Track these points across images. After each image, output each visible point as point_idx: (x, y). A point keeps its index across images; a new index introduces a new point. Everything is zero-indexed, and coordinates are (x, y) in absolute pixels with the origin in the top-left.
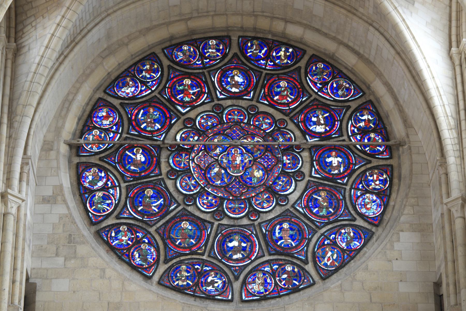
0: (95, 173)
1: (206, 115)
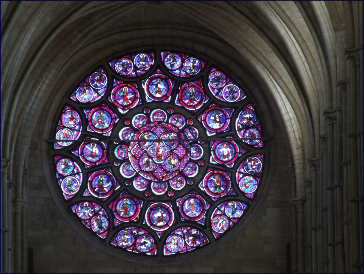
0: (66, 162)
1: (139, 116)
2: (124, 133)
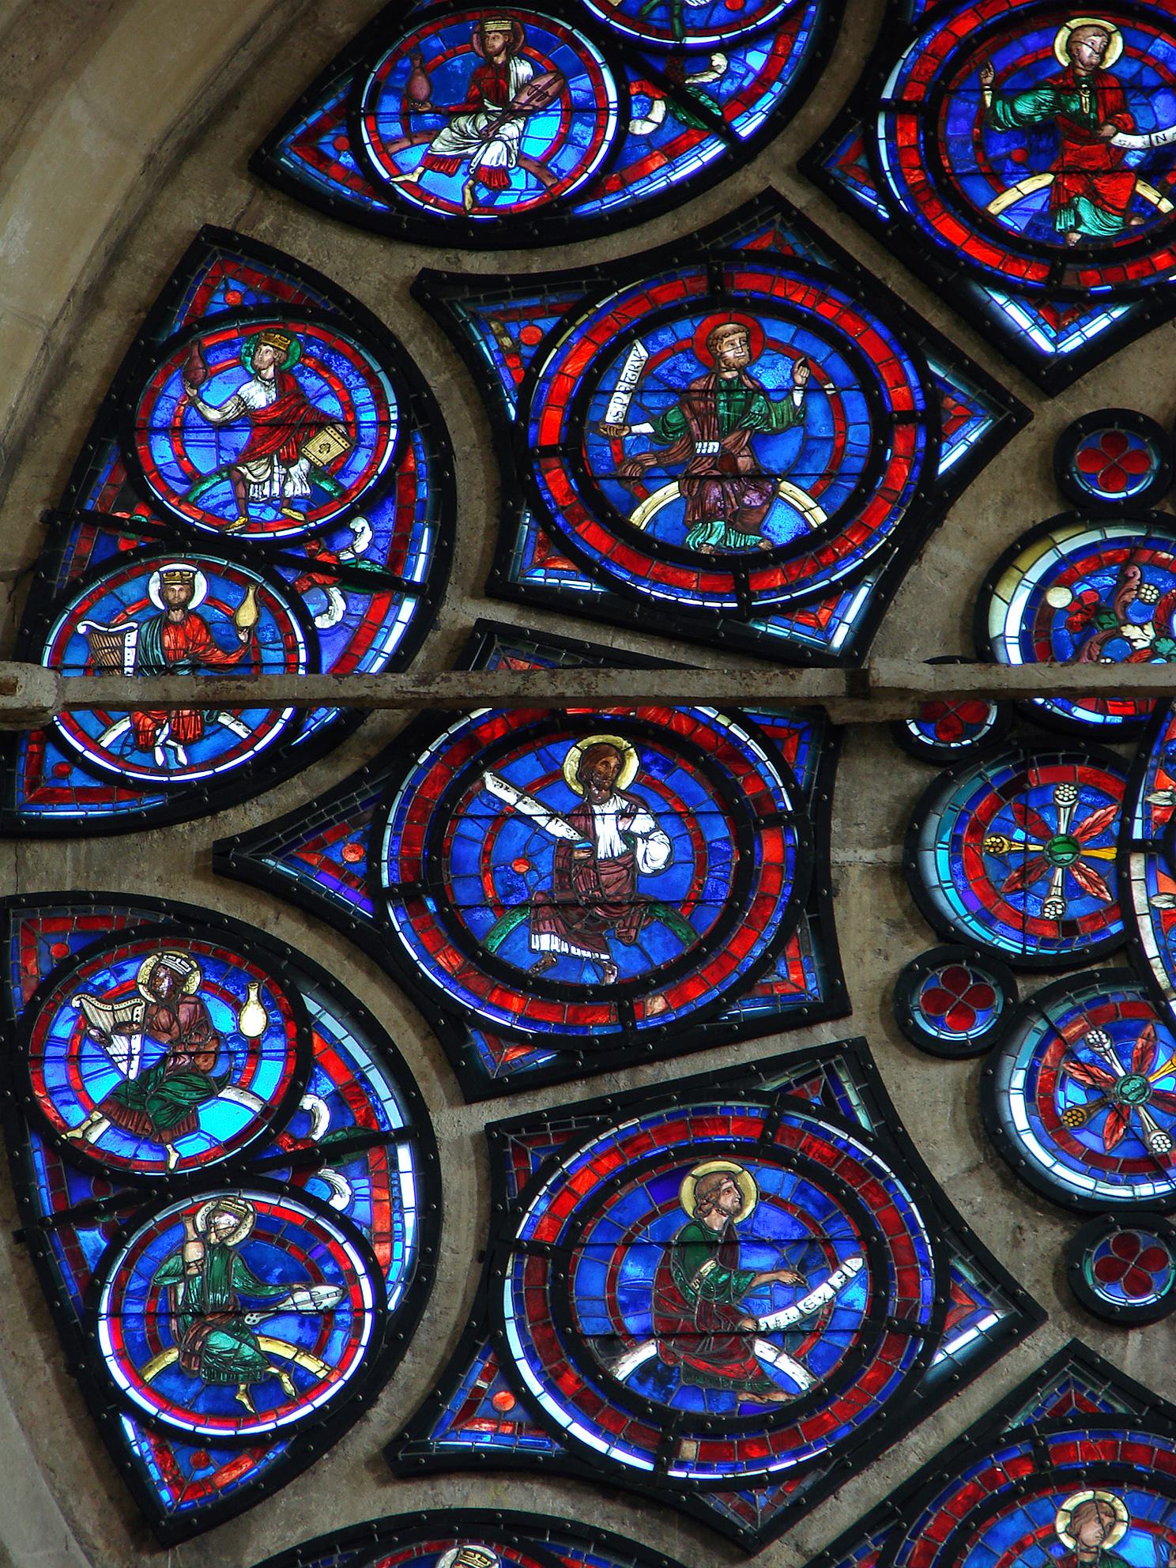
2: (1059, 598)
